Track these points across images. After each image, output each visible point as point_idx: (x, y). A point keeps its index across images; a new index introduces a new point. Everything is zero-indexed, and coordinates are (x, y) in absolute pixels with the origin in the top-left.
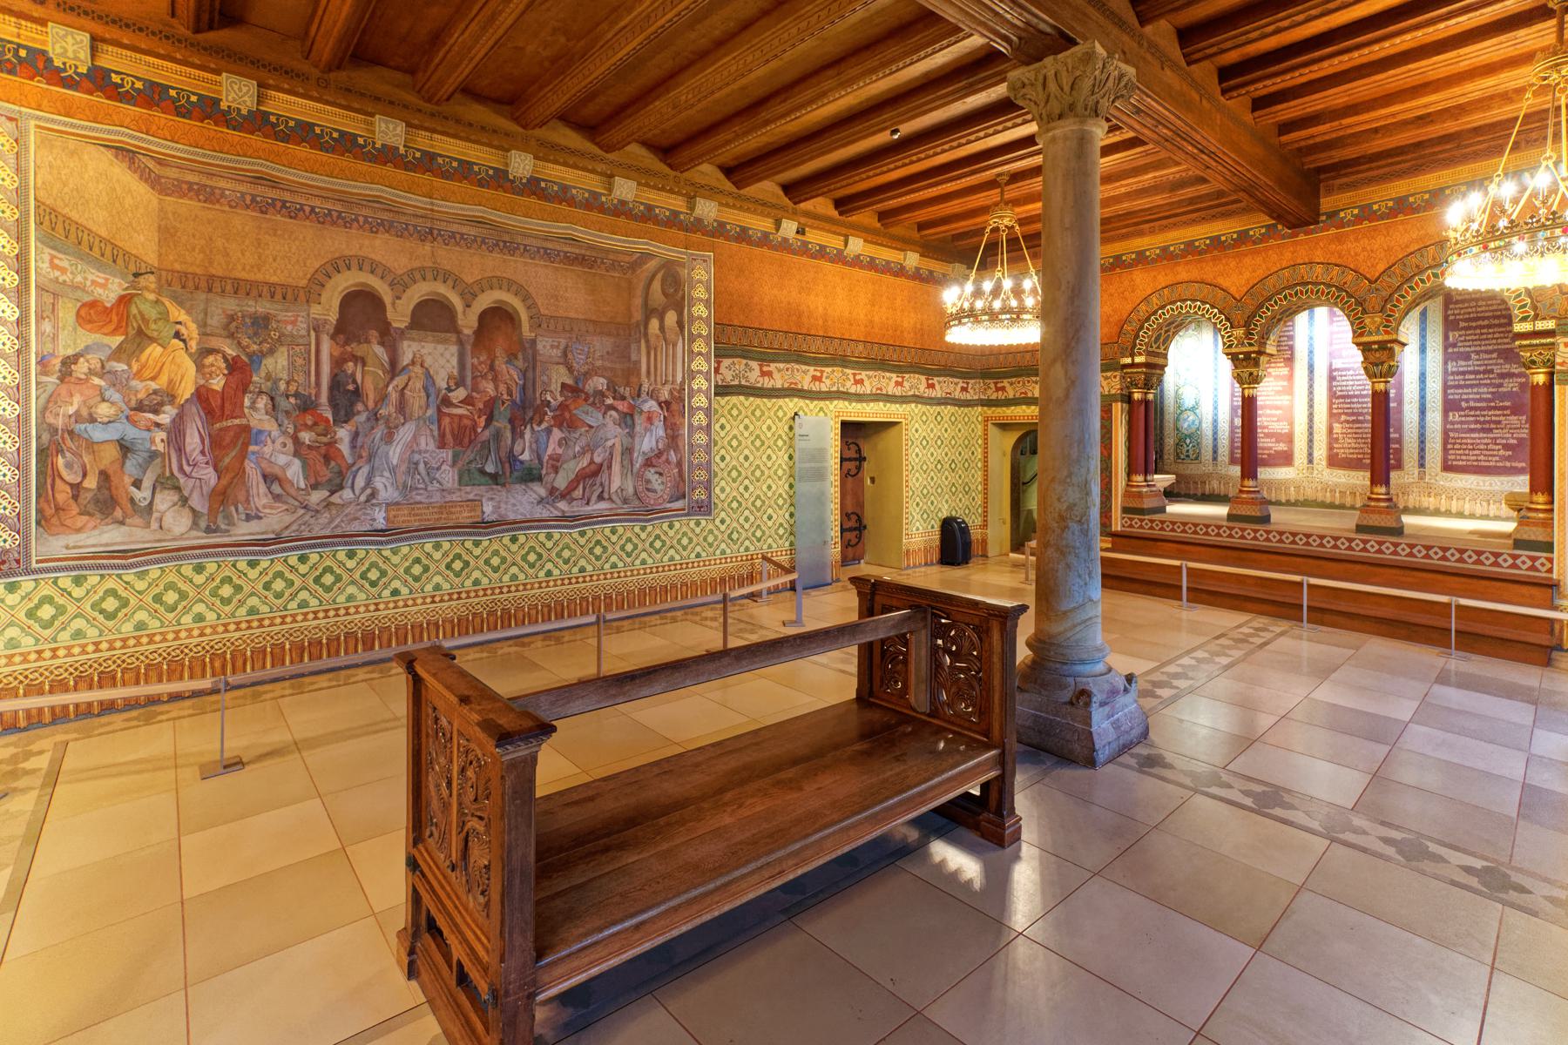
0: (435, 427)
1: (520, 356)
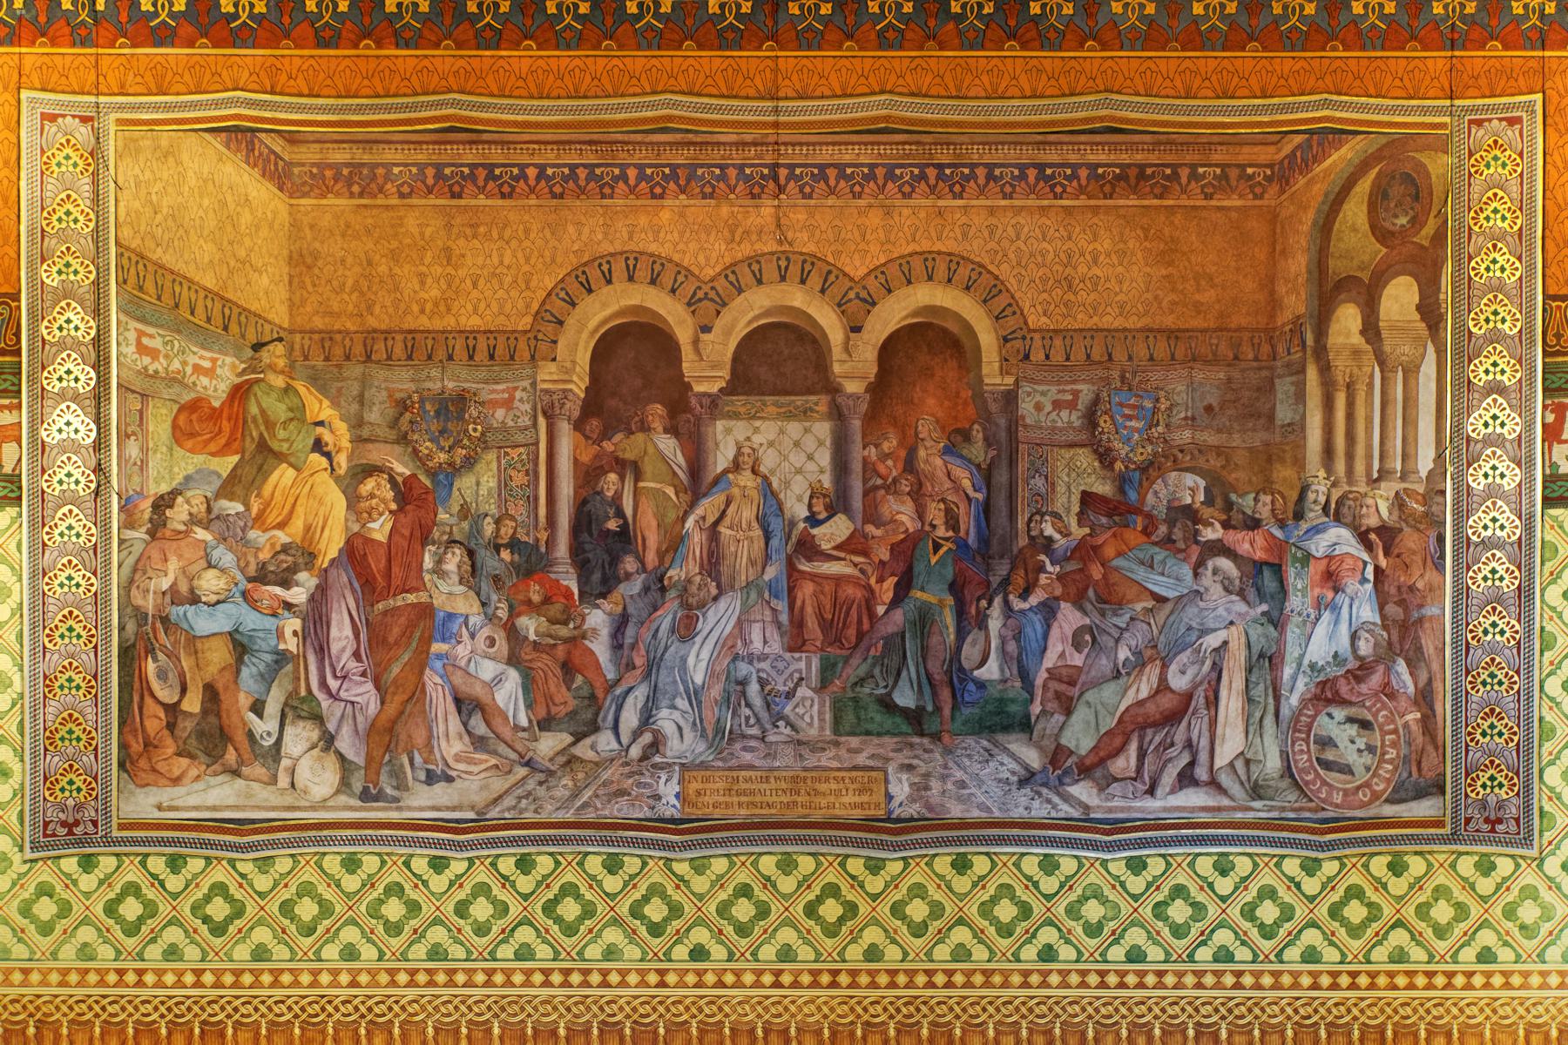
0: (782, 605)
1: (978, 434)
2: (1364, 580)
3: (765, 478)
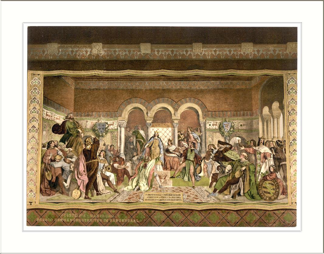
2: (271, 157)
3: (160, 138)
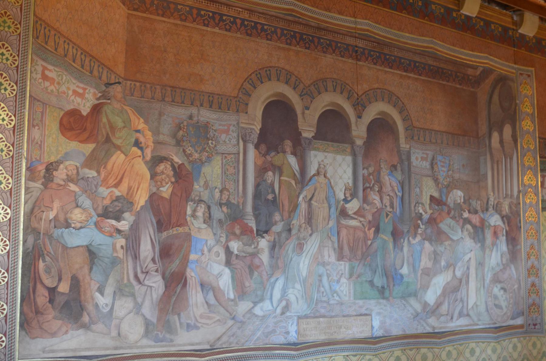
0: (335, 239)
1: (399, 168)
2: (503, 235)
3: (329, 180)
